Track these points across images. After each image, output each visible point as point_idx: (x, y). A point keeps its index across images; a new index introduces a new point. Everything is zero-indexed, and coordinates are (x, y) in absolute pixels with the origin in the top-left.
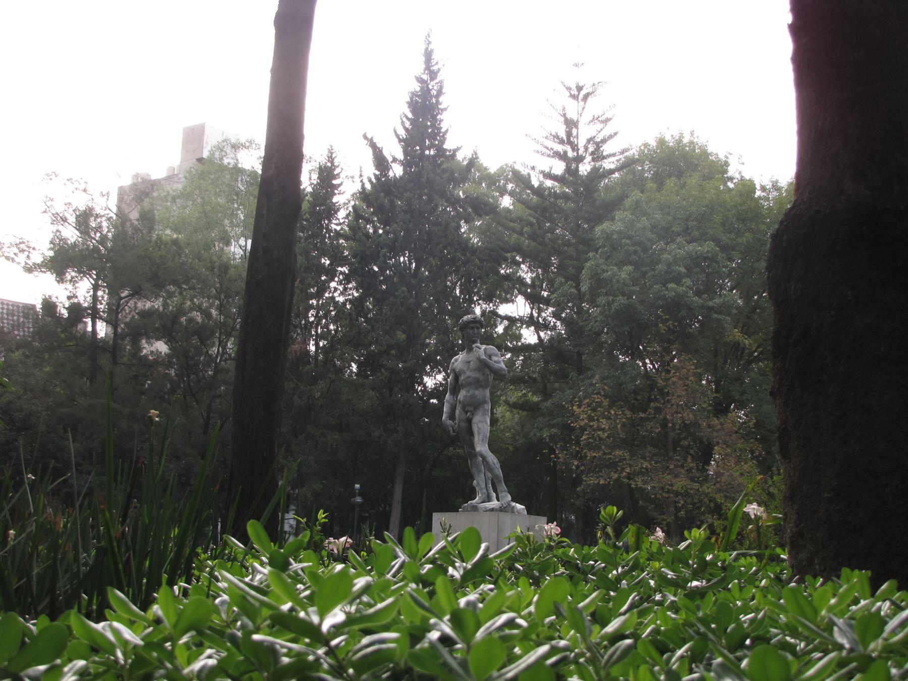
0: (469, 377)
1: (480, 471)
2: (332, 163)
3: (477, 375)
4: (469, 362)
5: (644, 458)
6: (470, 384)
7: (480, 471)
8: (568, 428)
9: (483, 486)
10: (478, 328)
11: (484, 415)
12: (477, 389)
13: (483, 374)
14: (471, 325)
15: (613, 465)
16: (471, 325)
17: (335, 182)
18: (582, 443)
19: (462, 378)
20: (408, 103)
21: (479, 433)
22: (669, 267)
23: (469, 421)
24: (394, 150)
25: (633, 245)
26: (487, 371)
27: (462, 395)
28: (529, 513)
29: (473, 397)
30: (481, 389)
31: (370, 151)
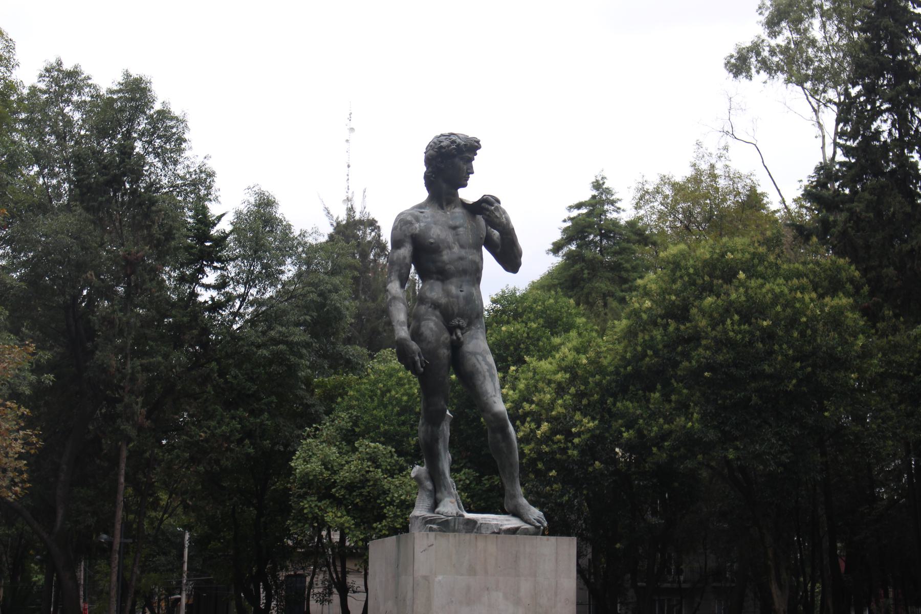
0: (461, 259)
23: (456, 347)
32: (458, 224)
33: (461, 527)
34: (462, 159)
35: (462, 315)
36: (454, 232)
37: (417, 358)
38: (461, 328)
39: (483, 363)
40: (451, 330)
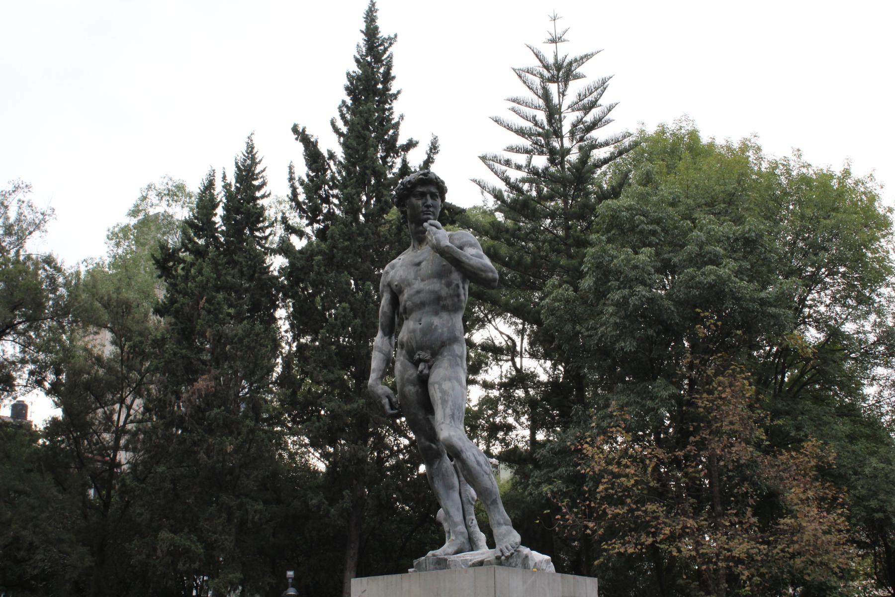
0: (418, 292)
1: (449, 487)
2: (253, 159)
3: (436, 285)
4: (419, 264)
5: (685, 513)
6: (422, 305)
7: (449, 487)
8: (577, 479)
9: (458, 517)
10: (433, 196)
11: (454, 365)
12: (436, 313)
13: (448, 285)
14: (420, 189)
15: (641, 527)
16: (420, 189)
17: (256, 183)
18: (598, 496)
19: (404, 298)
20: (347, 88)
21: (444, 402)
22: (701, 248)
24: (330, 144)
25: (651, 222)
26: (456, 277)
27: (408, 329)
28: (557, 571)
29: (428, 330)
30: (445, 315)
31: (300, 147)
32: (421, 258)
33: (432, 566)
34: (415, 196)
35: (422, 348)
36: (417, 268)
37: (385, 401)
38: (426, 361)
39: (438, 391)
40: (416, 364)
